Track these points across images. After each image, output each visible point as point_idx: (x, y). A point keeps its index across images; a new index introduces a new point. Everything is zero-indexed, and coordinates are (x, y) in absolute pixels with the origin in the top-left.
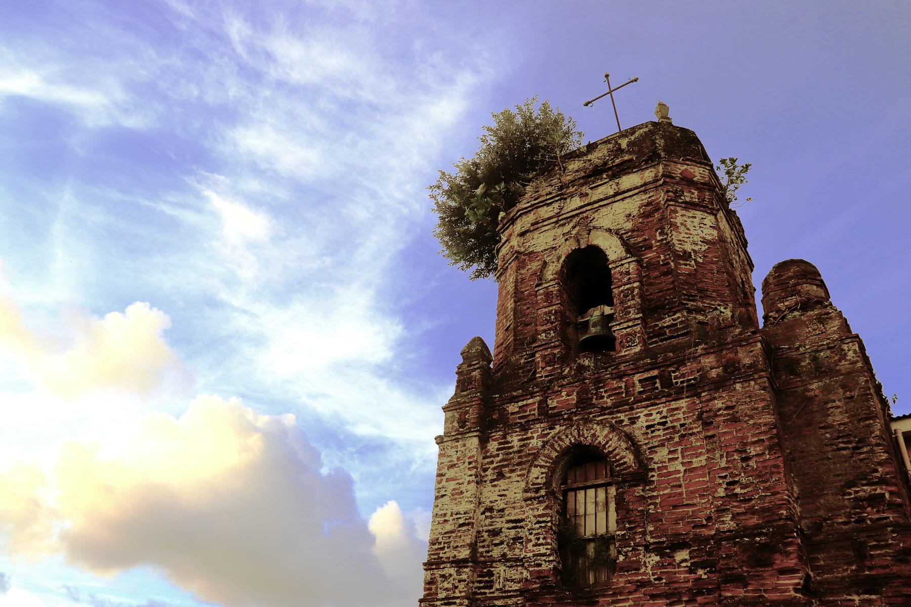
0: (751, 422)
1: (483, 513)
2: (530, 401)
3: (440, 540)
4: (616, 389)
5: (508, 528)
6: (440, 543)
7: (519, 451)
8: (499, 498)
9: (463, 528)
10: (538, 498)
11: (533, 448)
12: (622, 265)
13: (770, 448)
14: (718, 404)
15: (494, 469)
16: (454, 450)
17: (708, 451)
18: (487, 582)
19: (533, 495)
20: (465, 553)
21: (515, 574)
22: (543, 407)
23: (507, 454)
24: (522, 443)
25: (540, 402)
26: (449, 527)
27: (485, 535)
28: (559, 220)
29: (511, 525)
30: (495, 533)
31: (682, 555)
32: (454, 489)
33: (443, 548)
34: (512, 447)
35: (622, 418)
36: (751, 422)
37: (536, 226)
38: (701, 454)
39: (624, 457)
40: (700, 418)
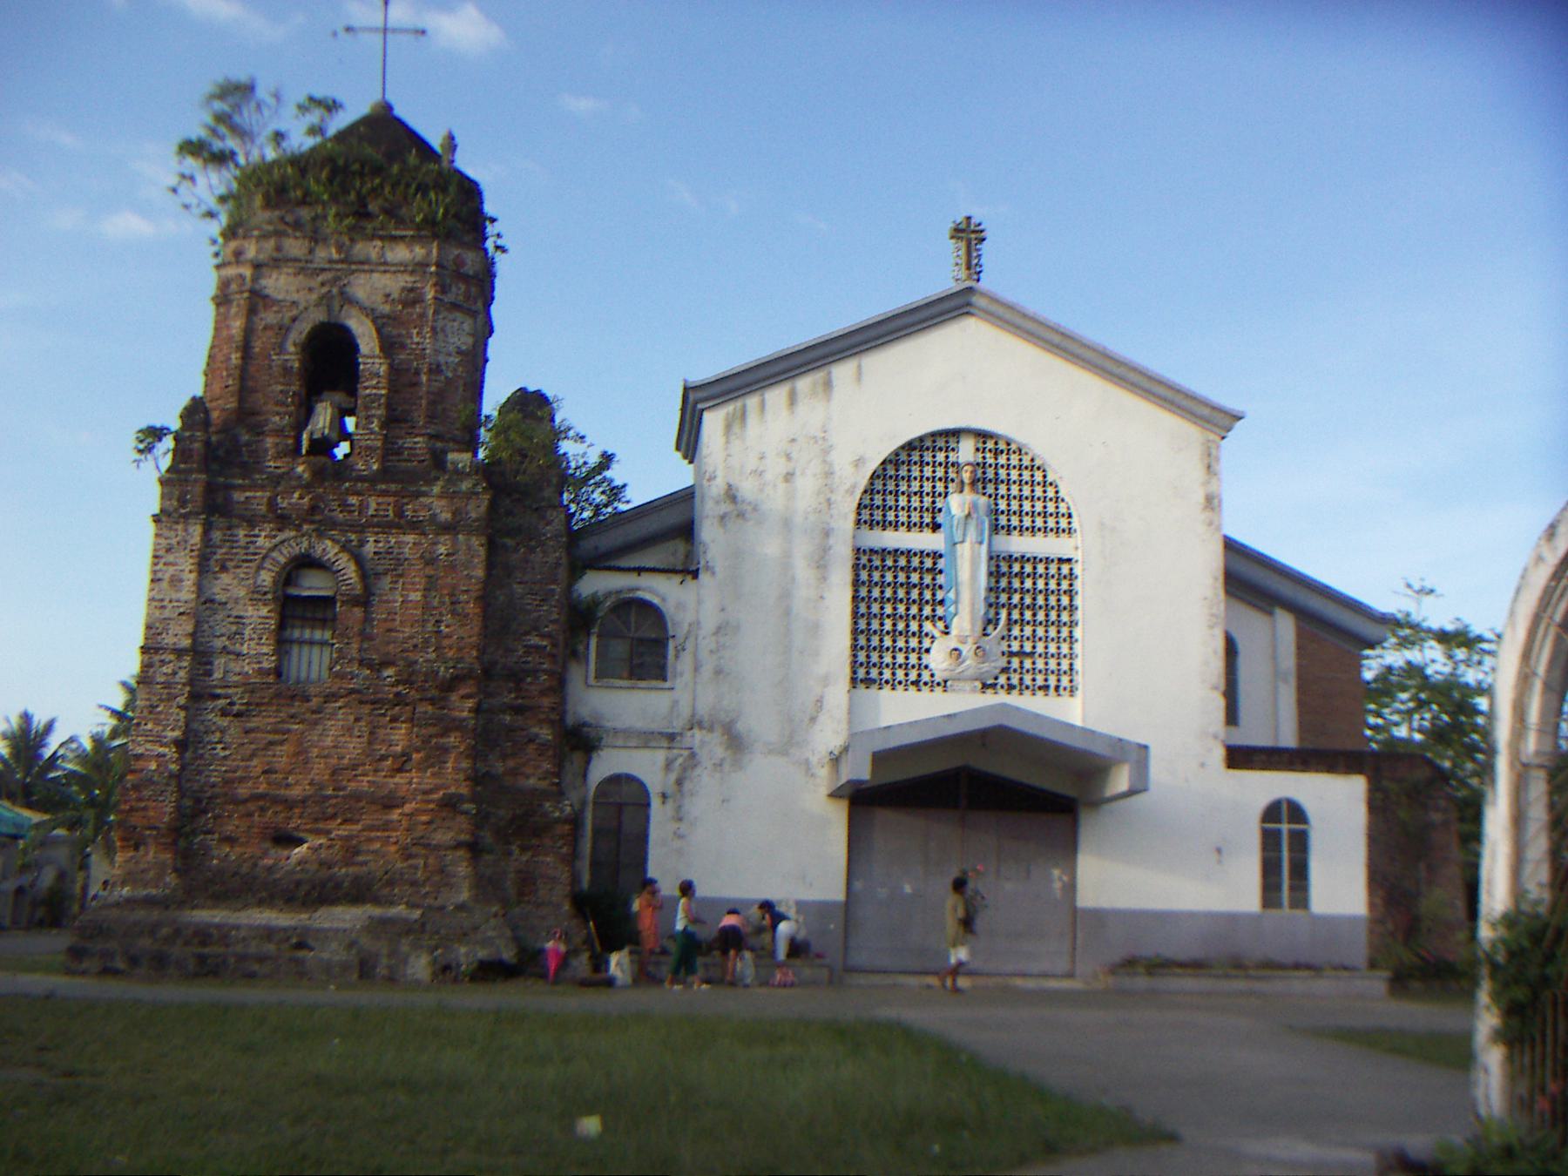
0: (465, 573)
2: (259, 494)
19: (260, 597)
22: (272, 503)
24: (249, 539)
25: (270, 498)
26: (167, 613)
28: (304, 268)
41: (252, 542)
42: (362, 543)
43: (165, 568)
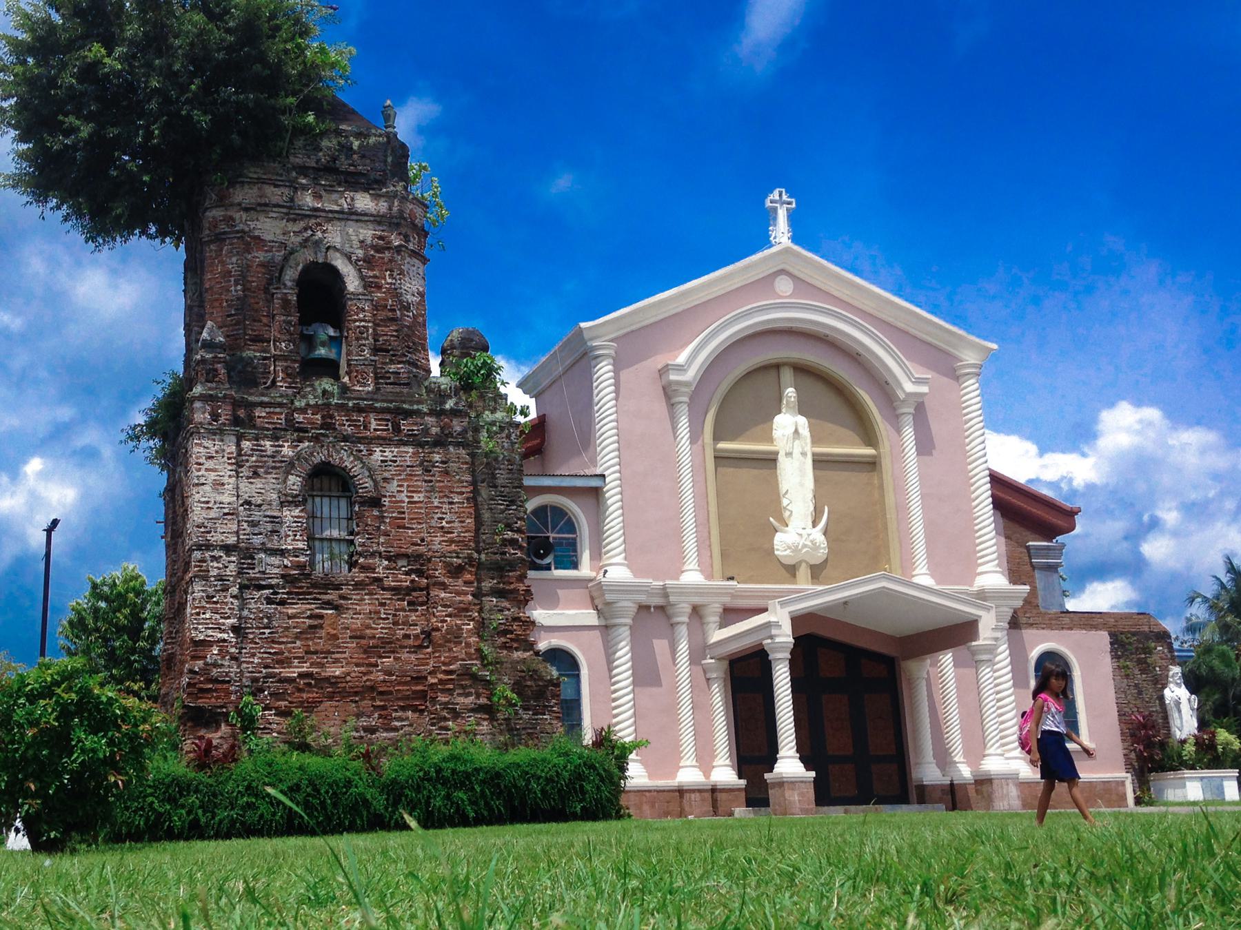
0: (457, 477)
1: (242, 505)
4: (355, 421)
7: (273, 457)
9: (229, 517)
11: (283, 456)
13: (468, 499)
14: (437, 457)
15: (250, 467)
17: (427, 491)
18: (249, 564)
20: (232, 540)
21: (275, 560)
23: (262, 456)
24: (274, 449)
26: (212, 514)
27: (245, 525)
30: (253, 524)
35: (362, 448)
36: (457, 477)
37: (263, 208)
38: (420, 492)
40: (421, 464)
41: (277, 452)
42: (371, 452)
43: (206, 474)
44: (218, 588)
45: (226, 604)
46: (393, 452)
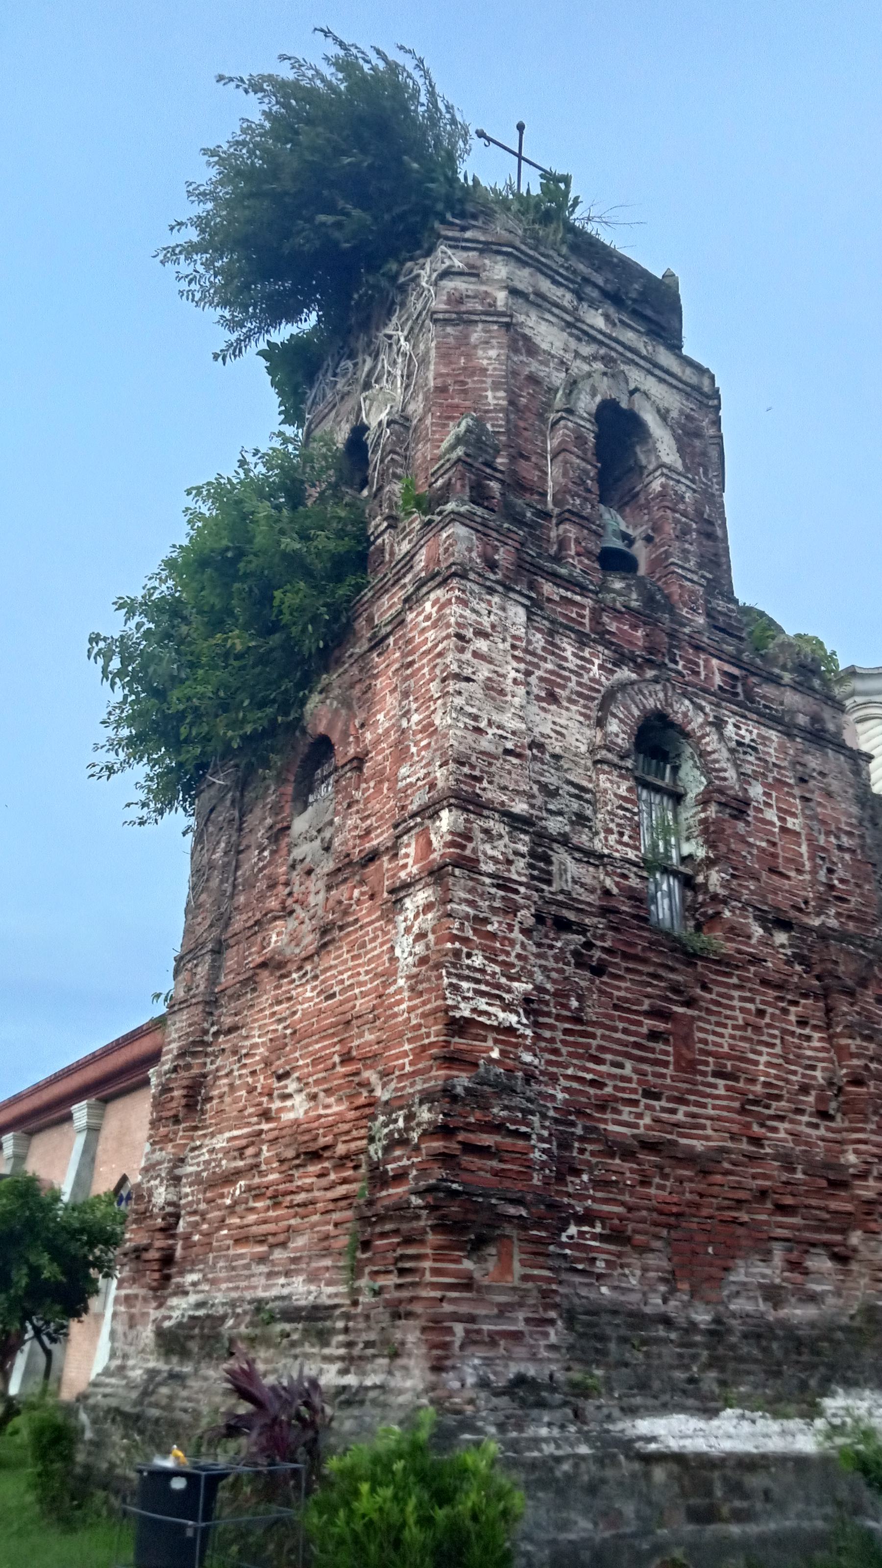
3: (473, 759)
5: (568, 794)
6: (473, 767)
8: (553, 735)
10: (621, 768)
12: (678, 482)
15: (541, 679)
16: (484, 605)
19: (616, 760)
26: (485, 743)
29: (573, 791)
31: (781, 938)
32: (489, 679)
33: (479, 779)
34: (565, 659)
37: (539, 301)
39: (725, 770)
41: (582, 667)
44: (497, 904)
45: (512, 943)
46: (751, 732)
